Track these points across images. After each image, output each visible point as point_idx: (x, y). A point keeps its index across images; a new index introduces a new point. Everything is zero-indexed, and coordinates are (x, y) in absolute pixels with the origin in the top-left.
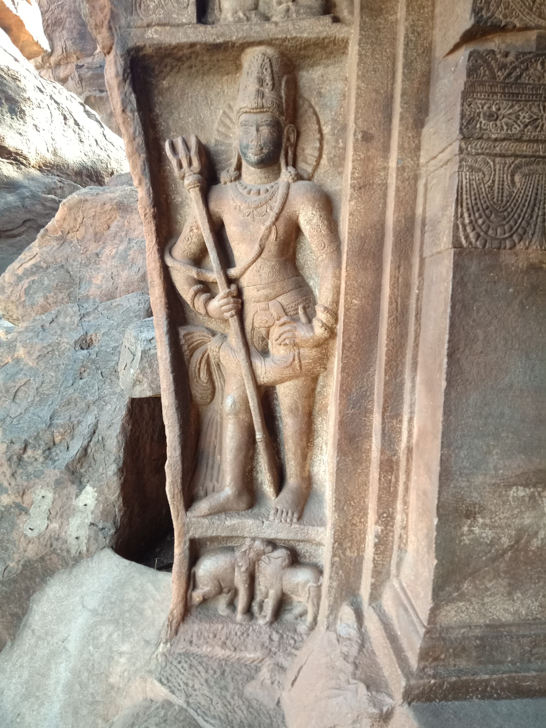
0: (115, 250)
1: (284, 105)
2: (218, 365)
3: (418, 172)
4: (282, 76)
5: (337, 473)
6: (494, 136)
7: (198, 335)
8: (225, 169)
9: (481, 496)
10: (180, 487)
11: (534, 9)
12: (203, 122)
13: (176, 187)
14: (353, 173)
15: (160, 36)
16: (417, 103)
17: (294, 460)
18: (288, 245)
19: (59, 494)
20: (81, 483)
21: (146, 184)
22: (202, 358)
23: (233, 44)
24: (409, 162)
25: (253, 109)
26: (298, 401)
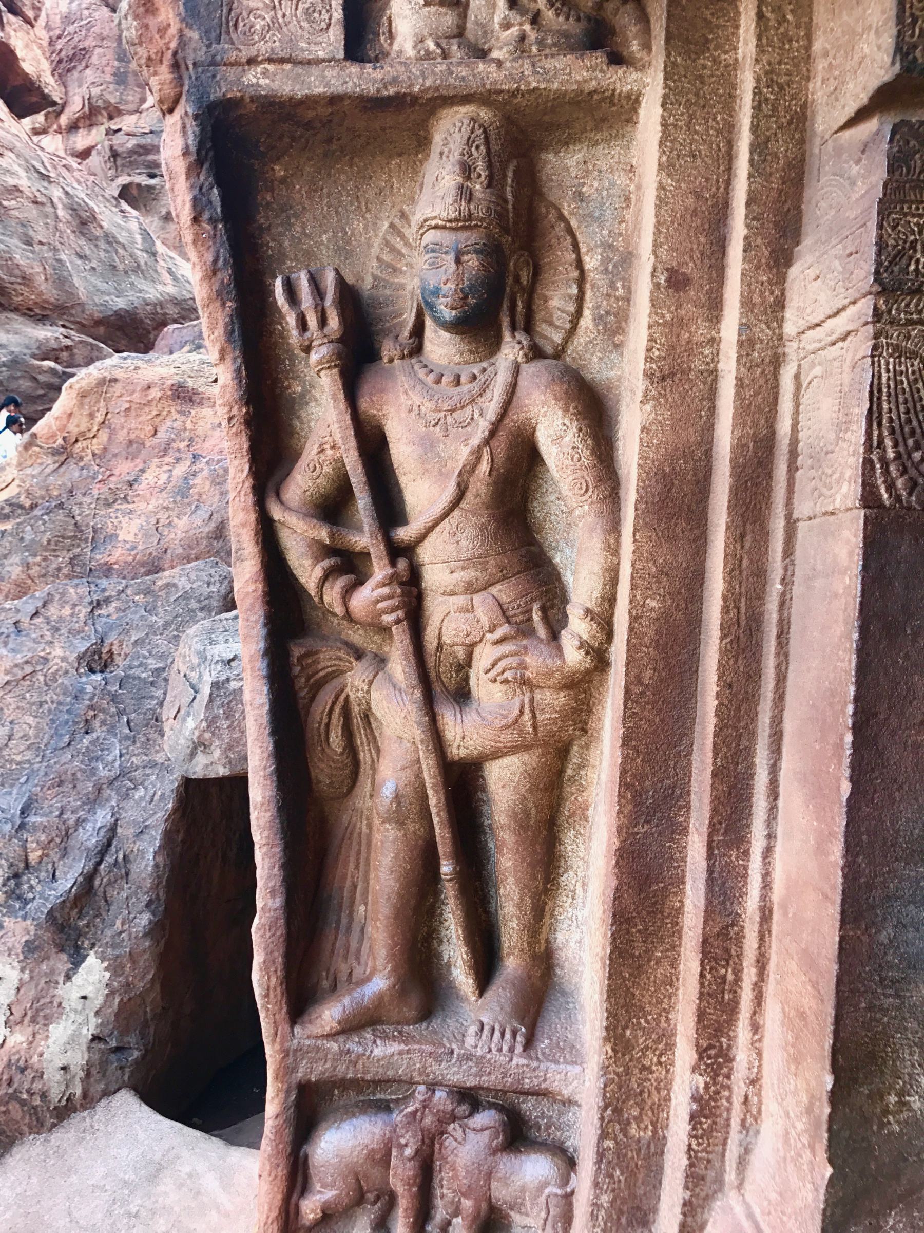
1: (511, 215)
2: (367, 716)
3: (780, 351)
5: (611, 959)
7: (327, 658)
8: (391, 332)
12: (349, 242)
13: (293, 365)
14: (649, 350)
15: (273, 81)
16: (778, 218)
17: (518, 918)
19: (31, 971)
20: (78, 948)
21: (235, 359)
22: (334, 703)
23: (415, 99)
24: (762, 331)
25: (450, 221)
26: (528, 796)
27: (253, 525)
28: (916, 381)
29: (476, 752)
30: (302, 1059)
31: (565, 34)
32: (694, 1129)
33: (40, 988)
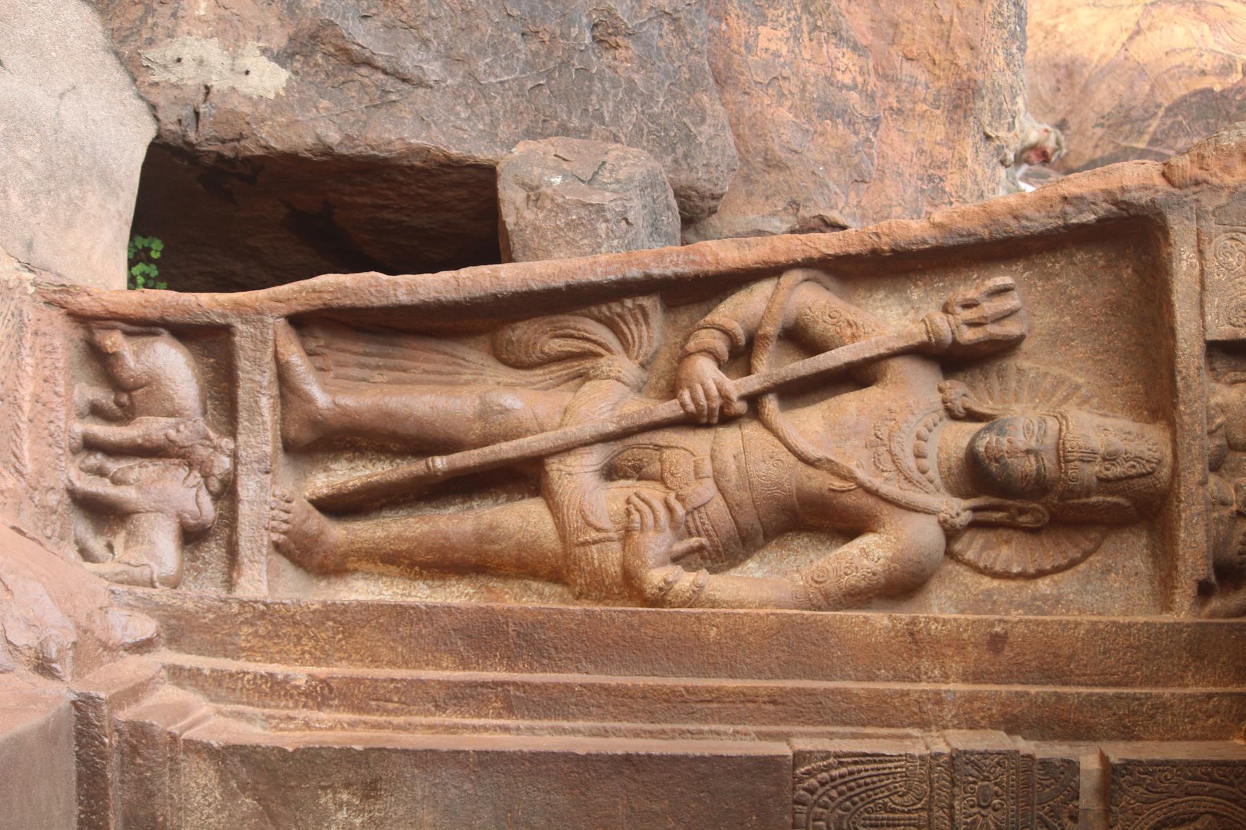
0: (847, 79)
3: (933, 727)
6: (956, 803)
10: (335, 303)
15: (1185, 274)
17: (387, 537)
18: (824, 517)
20: (292, 56)
22: (595, 342)
23: (1174, 406)
26: (512, 542)
27: (773, 259)
28: (889, 790)
29: (556, 487)
30: (255, 327)
31: (1226, 542)
32: (262, 676)
33: (253, 20)
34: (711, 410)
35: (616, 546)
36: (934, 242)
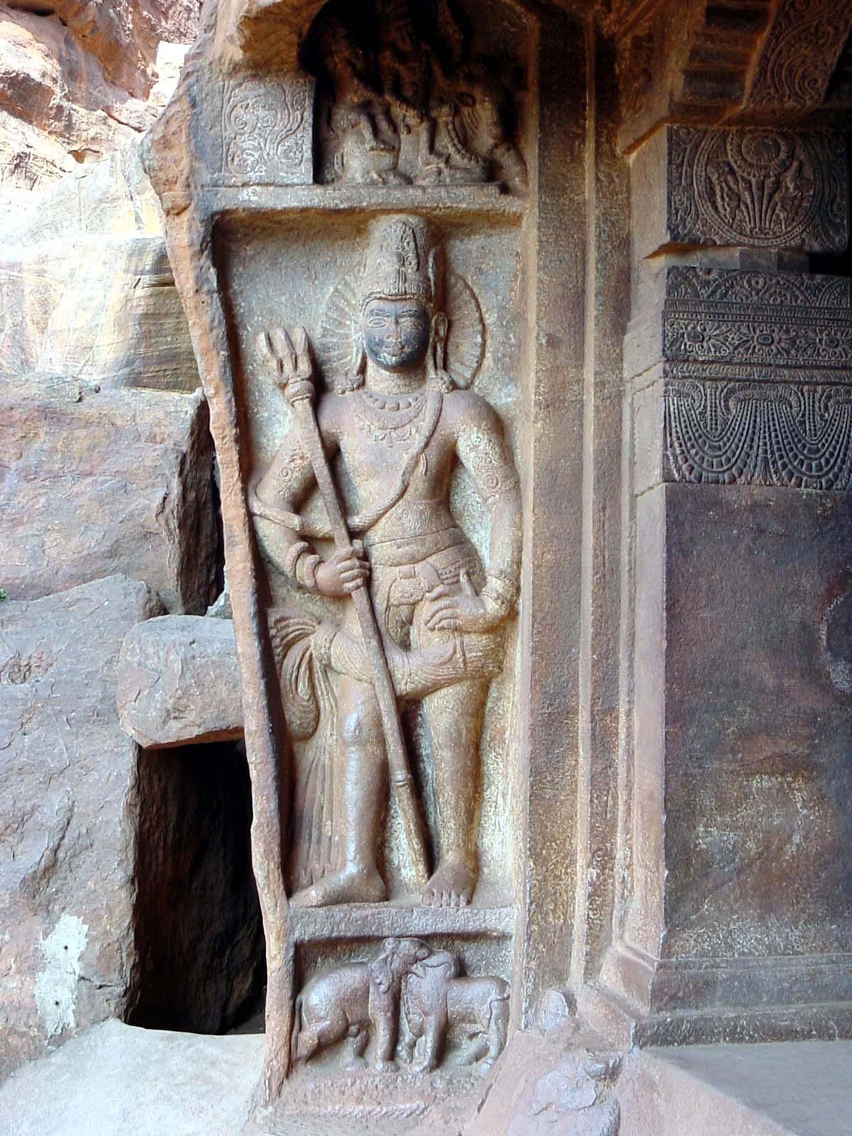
1: (433, 289)
4: (429, 251)
9: (718, 787)
10: (277, 859)
11: (734, 226)
14: (538, 387)
15: (260, 198)
17: (455, 819)
23: (362, 210)
26: (461, 720)
29: (420, 686)
30: (297, 924)
34: (361, 567)
35: (466, 638)
36: (230, 394)
